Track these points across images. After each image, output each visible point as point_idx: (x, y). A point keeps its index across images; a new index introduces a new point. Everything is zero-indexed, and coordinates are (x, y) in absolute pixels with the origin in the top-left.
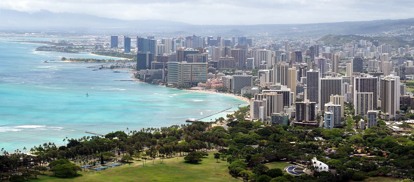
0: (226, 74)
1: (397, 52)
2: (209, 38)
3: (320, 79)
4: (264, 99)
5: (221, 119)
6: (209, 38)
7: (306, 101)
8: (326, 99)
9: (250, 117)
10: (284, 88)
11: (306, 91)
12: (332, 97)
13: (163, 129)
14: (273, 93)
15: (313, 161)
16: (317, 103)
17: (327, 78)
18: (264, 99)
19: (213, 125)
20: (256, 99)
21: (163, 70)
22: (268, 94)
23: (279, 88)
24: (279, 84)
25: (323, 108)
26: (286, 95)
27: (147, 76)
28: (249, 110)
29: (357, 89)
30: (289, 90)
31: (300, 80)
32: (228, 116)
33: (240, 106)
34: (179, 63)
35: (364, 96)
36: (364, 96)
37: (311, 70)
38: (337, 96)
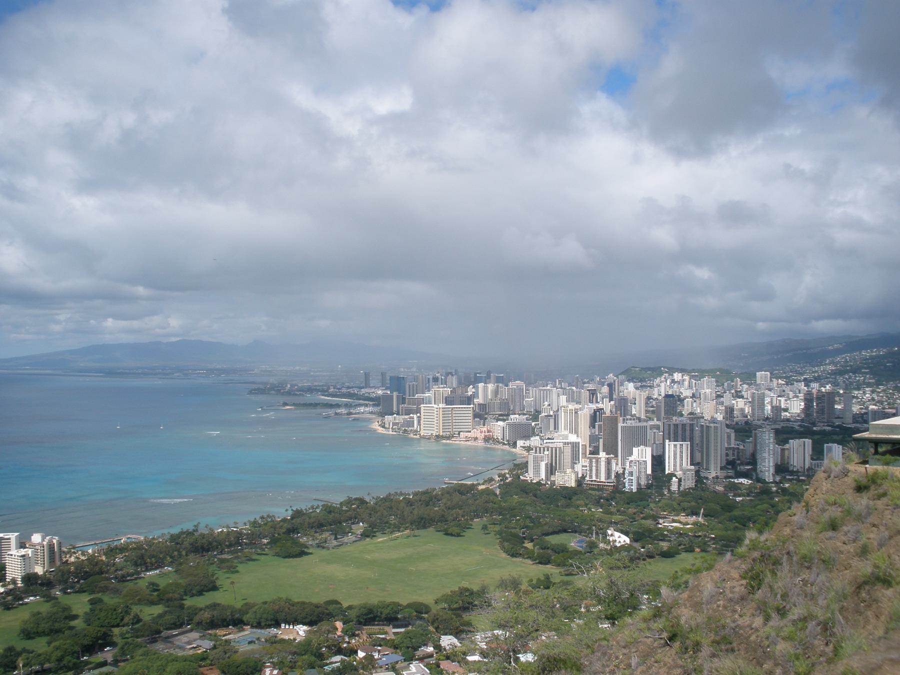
0: (498, 420)
2: (476, 374)
3: (620, 425)
4: (546, 453)
6: (476, 374)
7: (603, 455)
9: (530, 476)
10: (573, 438)
11: (601, 441)
12: (635, 450)
13: (415, 494)
14: (558, 442)
15: (610, 532)
16: (616, 456)
17: (630, 423)
18: (546, 453)
20: (536, 452)
21: (415, 416)
22: (551, 445)
23: (567, 438)
24: (566, 432)
25: (623, 464)
26: (575, 446)
27: (394, 424)
28: (527, 467)
30: (579, 440)
31: (594, 427)
34: (436, 406)
35: (678, 446)
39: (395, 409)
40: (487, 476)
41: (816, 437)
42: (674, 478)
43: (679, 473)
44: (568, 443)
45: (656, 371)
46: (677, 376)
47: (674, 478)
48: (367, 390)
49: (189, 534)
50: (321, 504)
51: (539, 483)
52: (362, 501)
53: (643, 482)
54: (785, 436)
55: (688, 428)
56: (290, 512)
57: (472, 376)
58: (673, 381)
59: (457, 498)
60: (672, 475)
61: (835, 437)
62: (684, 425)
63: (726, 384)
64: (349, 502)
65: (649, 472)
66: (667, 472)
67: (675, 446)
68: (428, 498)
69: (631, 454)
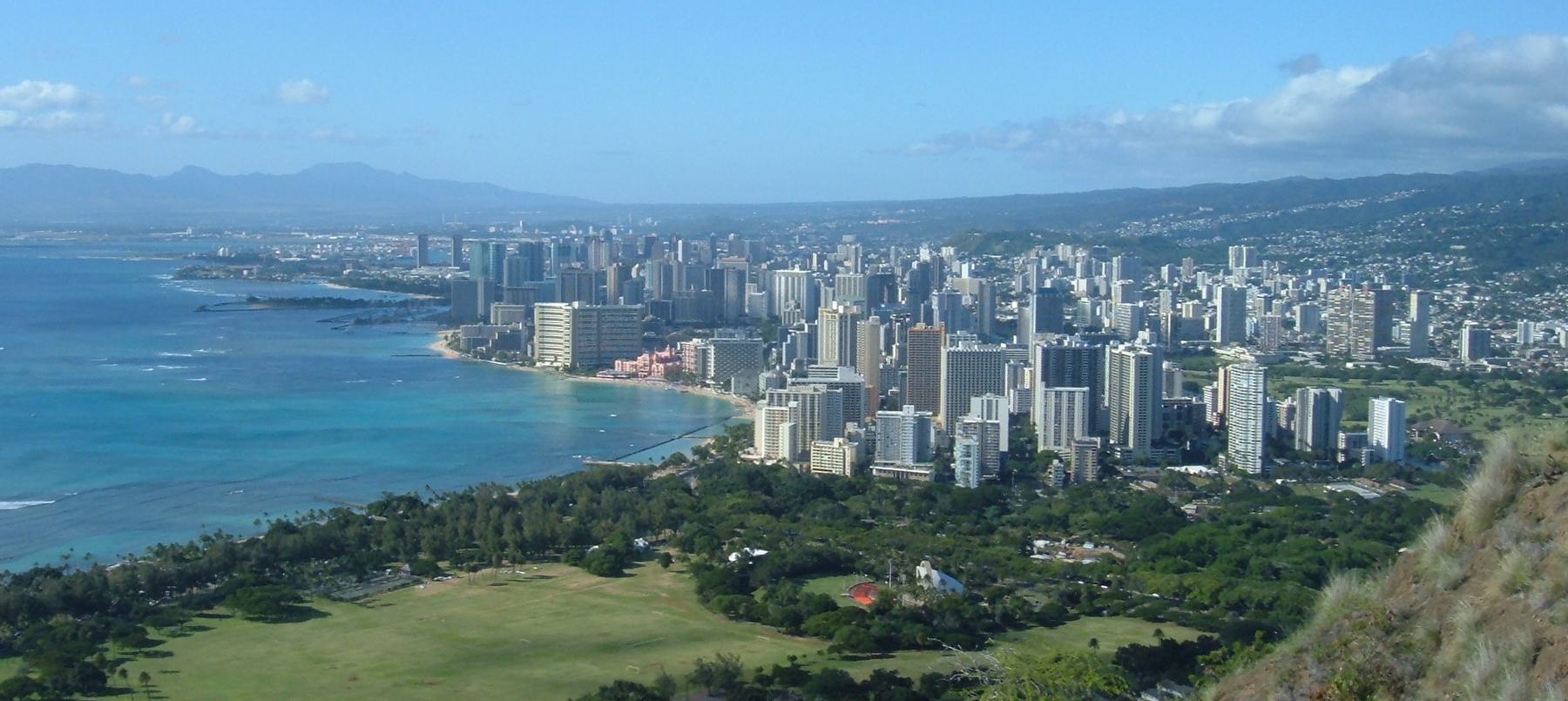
1: (1158, 277)
4: (793, 404)
5: (678, 459)
8: (959, 407)
10: (844, 375)
12: (976, 403)
13: (525, 487)
19: (656, 475)
29: (1045, 378)
32: (697, 451)
33: (730, 423)
35: (1065, 396)
36: (1065, 396)
37: (921, 326)
38: (989, 396)
39: (481, 311)
40: (667, 451)
41: (1355, 384)
42: (1056, 462)
43: (1063, 450)
44: (837, 386)
45: (1019, 240)
46: (1063, 251)
47: (1056, 462)
48: (424, 271)
49: (55, 573)
50: (327, 508)
51: (776, 468)
52: (413, 502)
53: (994, 465)
54: (1288, 379)
55: (1085, 359)
56: (265, 528)
57: (641, 242)
58: (1054, 262)
59: (607, 495)
60: (1050, 455)
61: (1392, 385)
62: (1077, 352)
63: (1165, 270)
64: (385, 506)
65: (1004, 446)
66: (1041, 448)
67: (1058, 394)
68: (552, 496)
69: (966, 409)
